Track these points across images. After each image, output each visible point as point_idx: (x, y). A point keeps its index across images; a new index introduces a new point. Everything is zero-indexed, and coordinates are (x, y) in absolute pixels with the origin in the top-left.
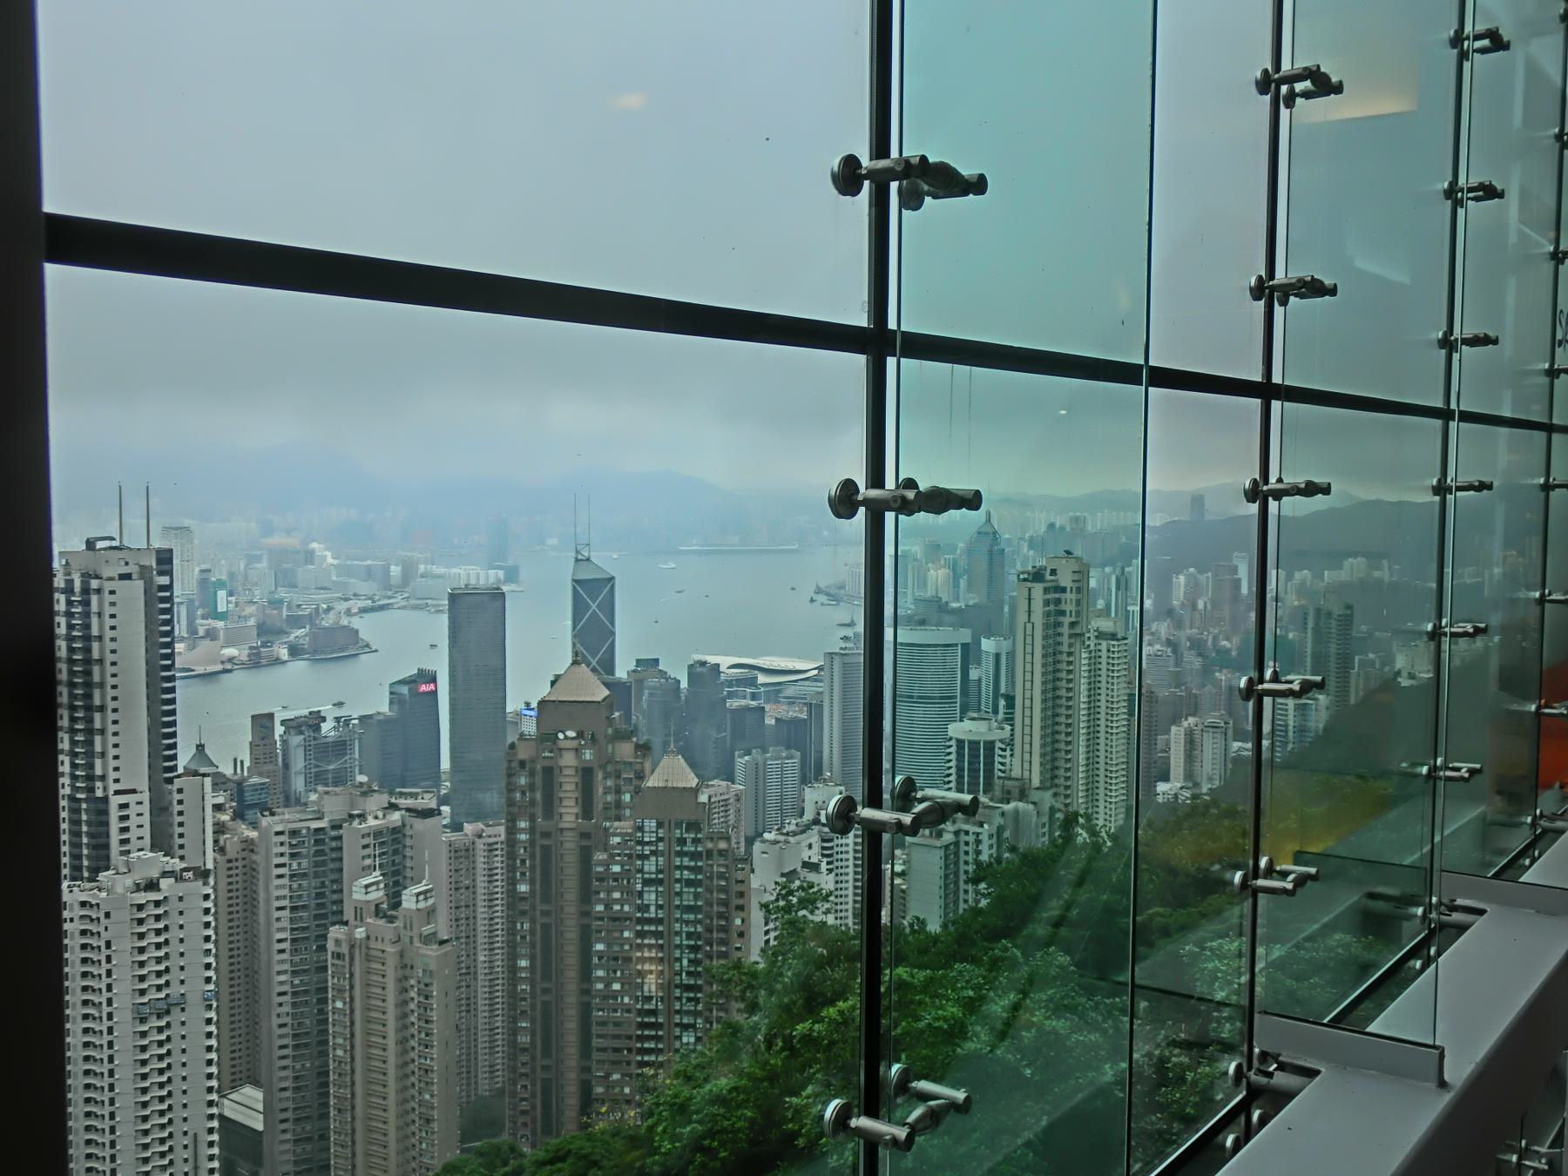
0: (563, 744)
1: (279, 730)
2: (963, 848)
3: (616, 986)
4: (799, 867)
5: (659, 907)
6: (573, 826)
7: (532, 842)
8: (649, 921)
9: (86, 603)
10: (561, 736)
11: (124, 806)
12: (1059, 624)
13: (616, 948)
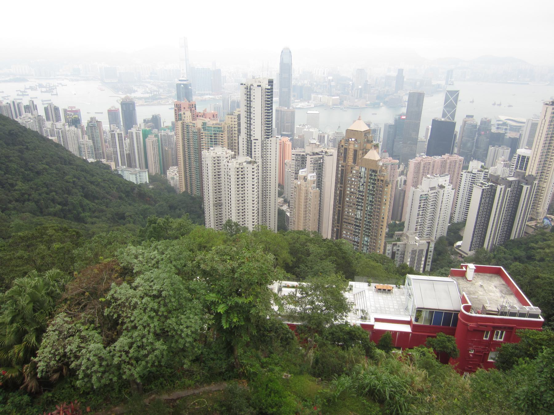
0: (350, 142)
3: (351, 210)
4: (437, 187)
6: (349, 165)
9: (250, 92)
10: (350, 140)
11: (255, 143)
13: (352, 200)
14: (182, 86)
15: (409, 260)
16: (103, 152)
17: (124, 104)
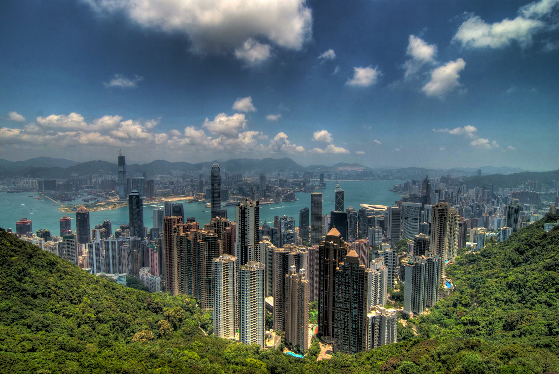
1: (279, 219)
2: (417, 267)
3: (340, 295)
5: (349, 281)
7: (324, 262)
8: (347, 283)
9: (244, 211)
11: (250, 248)
12: (442, 217)
14: (134, 197)
15: (386, 328)
16: (77, 261)
17: (79, 214)
